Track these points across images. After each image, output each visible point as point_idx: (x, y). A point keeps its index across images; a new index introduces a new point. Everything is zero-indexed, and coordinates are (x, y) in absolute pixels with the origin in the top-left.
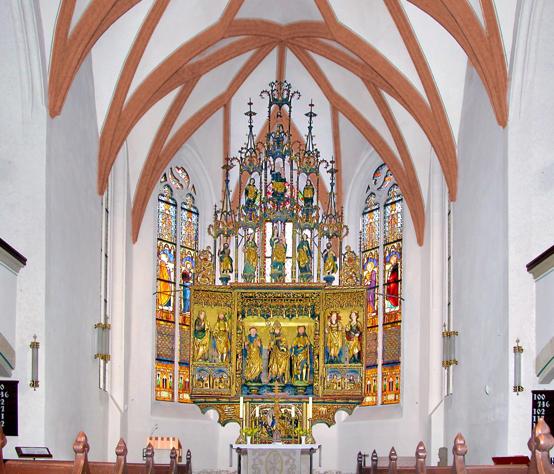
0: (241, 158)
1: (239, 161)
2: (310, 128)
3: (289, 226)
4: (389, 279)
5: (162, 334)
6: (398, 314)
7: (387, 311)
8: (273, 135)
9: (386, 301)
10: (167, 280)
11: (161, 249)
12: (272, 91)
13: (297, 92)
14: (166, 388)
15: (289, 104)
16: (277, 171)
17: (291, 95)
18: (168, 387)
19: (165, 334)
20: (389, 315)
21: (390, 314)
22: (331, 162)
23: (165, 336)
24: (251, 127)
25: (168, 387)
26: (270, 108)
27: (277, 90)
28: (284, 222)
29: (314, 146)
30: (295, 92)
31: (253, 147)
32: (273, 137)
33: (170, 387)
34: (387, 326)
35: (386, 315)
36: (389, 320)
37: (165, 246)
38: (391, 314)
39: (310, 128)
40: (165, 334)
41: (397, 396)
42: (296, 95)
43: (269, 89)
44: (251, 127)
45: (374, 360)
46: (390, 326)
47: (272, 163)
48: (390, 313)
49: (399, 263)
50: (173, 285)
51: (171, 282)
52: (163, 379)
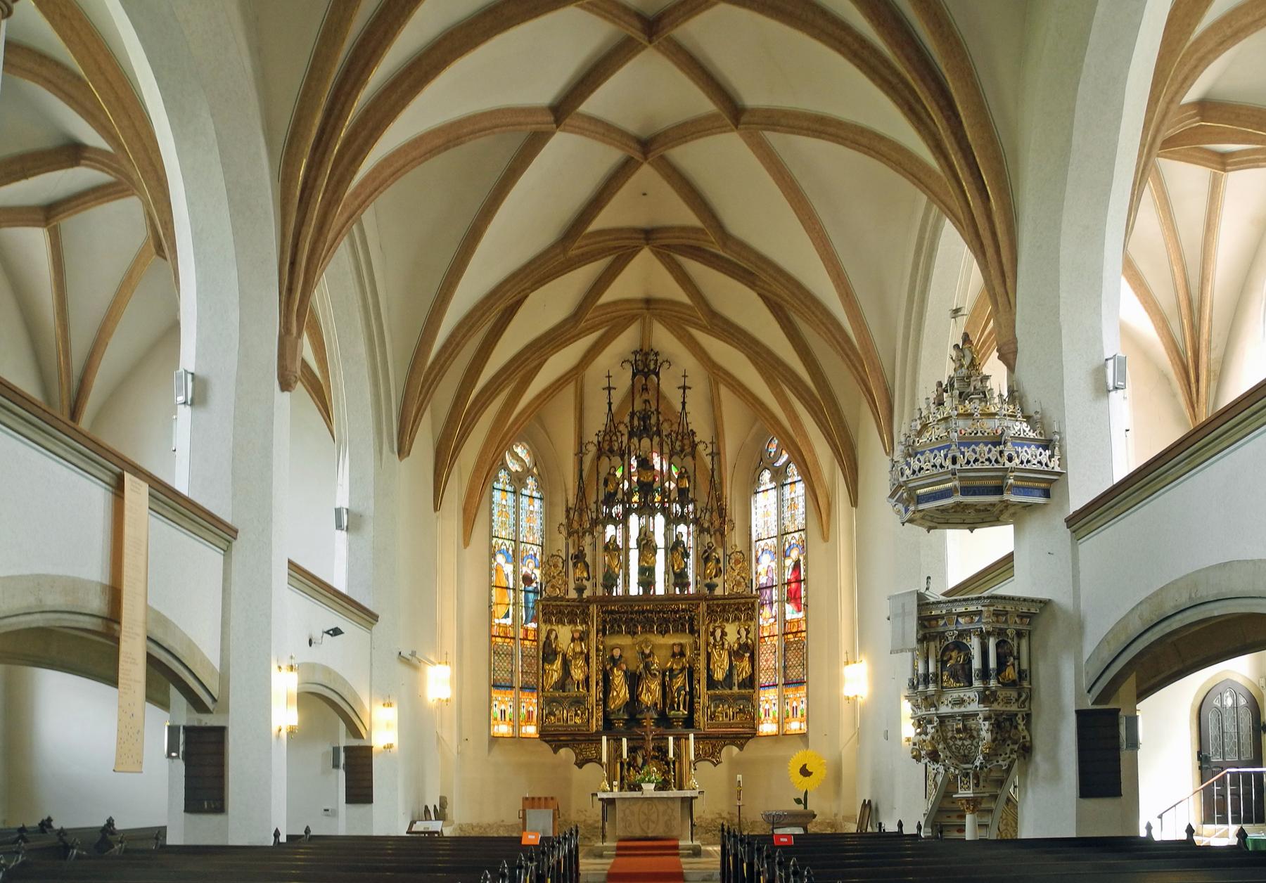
0: (599, 442)
1: (595, 445)
2: (684, 403)
3: (660, 520)
4: (789, 577)
5: (499, 653)
7: (788, 617)
8: (638, 414)
9: (786, 604)
10: (505, 586)
11: (497, 548)
12: (635, 360)
13: (667, 361)
14: (505, 720)
15: (657, 375)
17: (659, 364)
18: (507, 719)
19: (503, 653)
20: (790, 622)
21: (791, 622)
22: (710, 443)
23: (503, 656)
24: (610, 404)
25: (507, 719)
26: (633, 379)
27: (642, 361)
28: (652, 515)
29: (689, 425)
30: (664, 362)
31: (613, 429)
33: (510, 720)
37: (502, 544)
39: (684, 403)
40: (503, 653)
41: (802, 724)
42: (666, 365)
43: (632, 358)
44: (610, 404)
45: (774, 678)
47: (637, 447)
49: (801, 558)
50: (511, 591)
51: (510, 589)
52: (501, 711)
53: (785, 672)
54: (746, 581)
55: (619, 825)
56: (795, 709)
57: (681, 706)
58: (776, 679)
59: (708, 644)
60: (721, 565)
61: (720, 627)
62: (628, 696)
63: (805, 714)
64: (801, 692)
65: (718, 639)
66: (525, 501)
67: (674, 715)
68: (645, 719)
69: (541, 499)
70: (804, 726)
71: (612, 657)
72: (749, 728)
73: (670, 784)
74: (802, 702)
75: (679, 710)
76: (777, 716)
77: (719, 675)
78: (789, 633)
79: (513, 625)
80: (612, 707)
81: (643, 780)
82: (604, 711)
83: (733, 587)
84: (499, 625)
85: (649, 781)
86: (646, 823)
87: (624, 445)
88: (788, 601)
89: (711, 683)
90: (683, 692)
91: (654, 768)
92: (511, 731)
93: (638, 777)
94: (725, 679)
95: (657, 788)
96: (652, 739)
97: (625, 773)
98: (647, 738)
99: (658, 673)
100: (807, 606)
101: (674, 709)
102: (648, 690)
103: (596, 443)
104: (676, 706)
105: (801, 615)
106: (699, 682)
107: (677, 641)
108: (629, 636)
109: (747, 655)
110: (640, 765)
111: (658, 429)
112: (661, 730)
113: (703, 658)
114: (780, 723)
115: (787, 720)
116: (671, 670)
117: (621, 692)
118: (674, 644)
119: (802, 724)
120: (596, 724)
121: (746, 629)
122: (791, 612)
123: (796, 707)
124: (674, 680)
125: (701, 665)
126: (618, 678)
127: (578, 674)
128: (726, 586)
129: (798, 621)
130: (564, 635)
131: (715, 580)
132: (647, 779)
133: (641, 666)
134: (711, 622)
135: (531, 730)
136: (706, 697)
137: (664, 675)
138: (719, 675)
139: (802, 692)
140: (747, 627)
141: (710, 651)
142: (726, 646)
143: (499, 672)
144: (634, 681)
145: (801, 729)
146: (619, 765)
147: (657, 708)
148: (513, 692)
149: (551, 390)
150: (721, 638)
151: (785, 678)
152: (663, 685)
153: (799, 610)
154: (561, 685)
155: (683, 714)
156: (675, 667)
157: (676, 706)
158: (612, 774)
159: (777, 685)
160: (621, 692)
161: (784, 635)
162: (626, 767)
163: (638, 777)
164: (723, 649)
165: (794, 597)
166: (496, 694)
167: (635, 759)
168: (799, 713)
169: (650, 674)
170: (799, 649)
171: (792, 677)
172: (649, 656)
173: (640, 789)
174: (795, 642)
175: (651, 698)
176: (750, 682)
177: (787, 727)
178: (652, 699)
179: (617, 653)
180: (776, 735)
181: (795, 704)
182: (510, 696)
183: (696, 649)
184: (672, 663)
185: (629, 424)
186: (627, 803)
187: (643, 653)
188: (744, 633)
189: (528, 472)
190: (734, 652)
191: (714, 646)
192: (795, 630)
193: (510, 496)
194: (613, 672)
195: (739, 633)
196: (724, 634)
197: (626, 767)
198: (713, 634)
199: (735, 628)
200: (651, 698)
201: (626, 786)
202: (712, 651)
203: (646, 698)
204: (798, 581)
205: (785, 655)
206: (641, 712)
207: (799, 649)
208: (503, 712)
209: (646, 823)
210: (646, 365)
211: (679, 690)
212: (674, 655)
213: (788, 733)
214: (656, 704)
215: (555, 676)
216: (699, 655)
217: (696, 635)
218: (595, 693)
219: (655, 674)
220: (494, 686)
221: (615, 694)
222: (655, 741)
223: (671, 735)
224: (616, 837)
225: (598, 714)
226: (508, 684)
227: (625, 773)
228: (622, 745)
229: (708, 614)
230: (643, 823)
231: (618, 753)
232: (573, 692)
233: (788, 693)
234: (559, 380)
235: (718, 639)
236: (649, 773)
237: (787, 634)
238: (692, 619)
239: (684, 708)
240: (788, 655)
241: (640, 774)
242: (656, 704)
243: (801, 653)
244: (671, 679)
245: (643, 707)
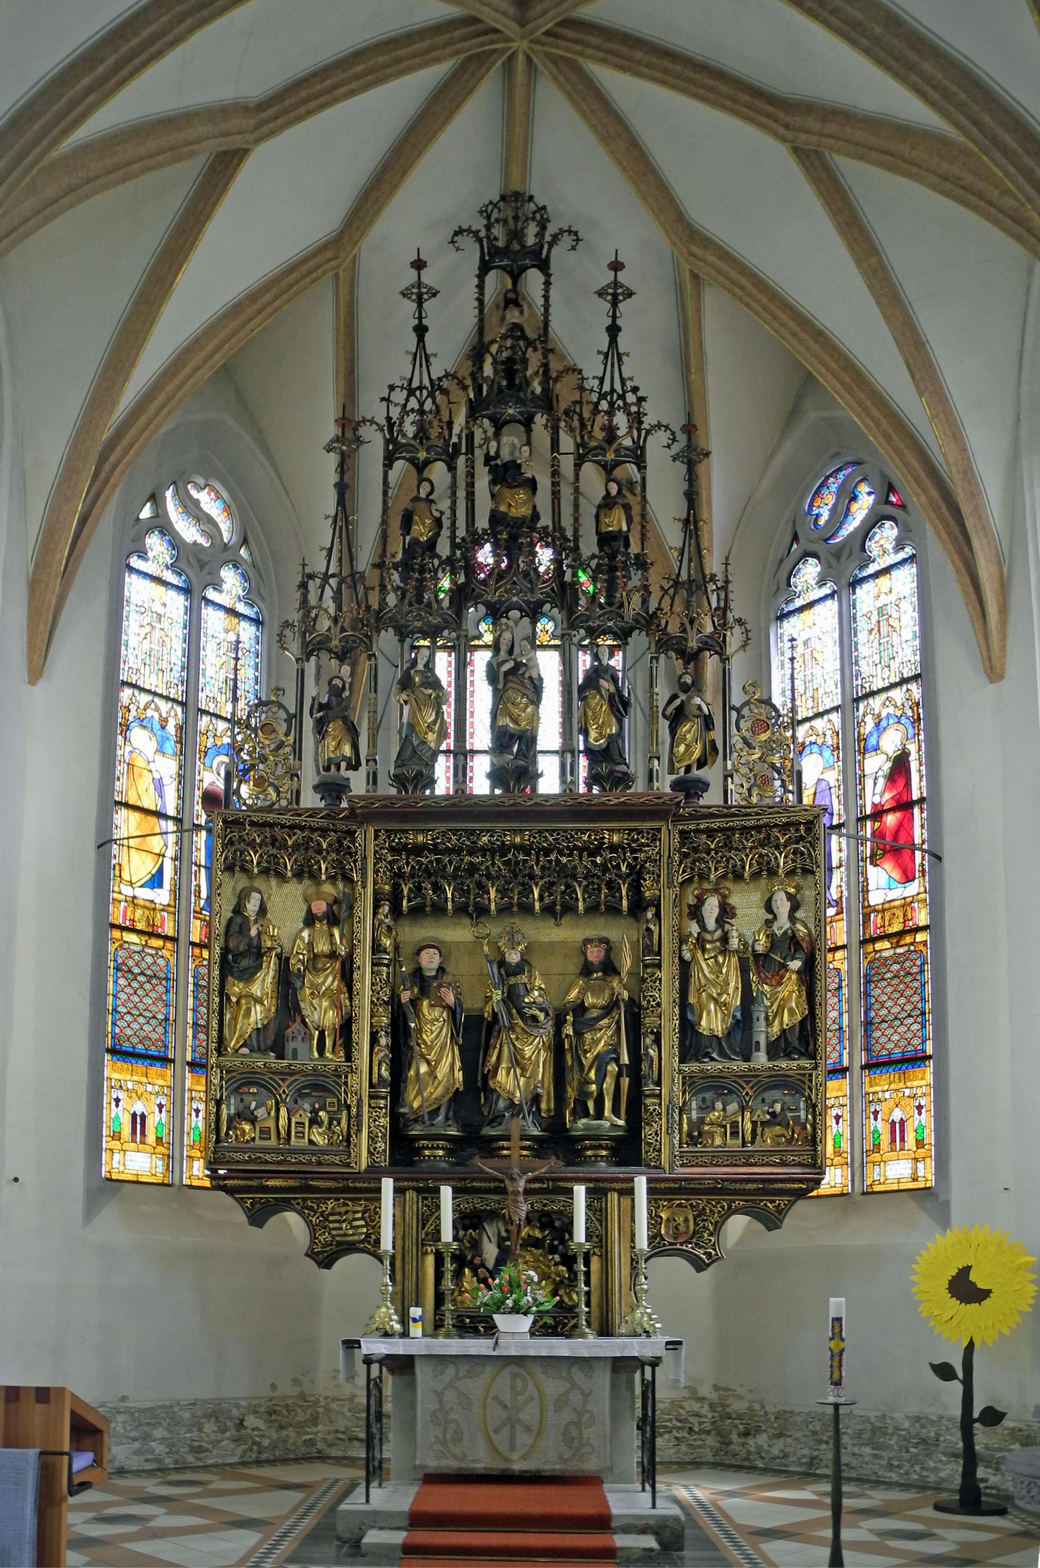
6: (916, 905)
16: (506, 456)
20: (883, 911)
32: (491, 354)
34: (879, 946)
35: (875, 911)
36: (884, 926)
38: (890, 909)
46: (886, 944)
48: (887, 906)
53: (868, 1035)
54: (784, 777)
55: (426, 1432)
56: (898, 1129)
57: (608, 1104)
58: (841, 1055)
59: (682, 941)
61: (716, 891)
62: (459, 1075)
63: (930, 1137)
64: (915, 1083)
65: (711, 923)
67: (587, 1128)
68: (507, 1138)
70: (927, 1172)
71: (418, 972)
73: (576, 1316)
74: (920, 1108)
75: (599, 1115)
76: (846, 1146)
78: (880, 938)
80: (416, 1105)
81: (498, 1306)
83: (749, 790)
85: (516, 1310)
86: (506, 1430)
87: (456, 430)
90: (612, 1068)
91: (532, 1273)
92: (160, 1169)
93: (485, 1296)
95: (541, 1329)
96: (527, 1192)
97: (448, 1283)
98: (510, 1188)
99: (541, 1016)
100: (939, 858)
101: (587, 1114)
102: (517, 1061)
103: (383, 422)
104: (591, 1104)
105: (913, 888)
106: (657, 1041)
107: (590, 933)
108: (467, 921)
110: (490, 1263)
111: (546, 390)
112: (550, 1165)
113: (668, 973)
114: (857, 1164)
115: (876, 1157)
116: (580, 1009)
118: (587, 941)
119: (921, 1166)
121: (790, 897)
123: (902, 1122)
124: (588, 1036)
125: (666, 993)
128: (730, 786)
129: (907, 904)
132: (509, 1303)
133: (497, 995)
134: (690, 881)
135: (197, 1171)
136: (678, 1079)
137: (559, 1023)
139: (924, 1078)
140: (792, 890)
141: (687, 956)
142: (734, 943)
143: (128, 1018)
145: (915, 1179)
146: (430, 1261)
147: (539, 1110)
148: (169, 1072)
149: (268, 296)
150: (720, 921)
151: (868, 1050)
152: (557, 1049)
153: (908, 877)
155: (614, 1126)
156: (590, 1000)
157: (591, 1104)
158: (411, 1285)
159: (847, 1069)
161: (864, 942)
162: (449, 1266)
163: (485, 1296)
164: (724, 952)
167: (476, 1246)
168: (910, 1138)
169: (522, 1015)
170: (909, 973)
171: (890, 1045)
172: (518, 969)
173: (491, 1330)
174: (896, 959)
175: (522, 1081)
177: (874, 1174)
178: (527, 1085)
179: (430, 960)
180: (842, 1195)
181: (897, 1115)
182: (161, 1082)
183: (648, 950)
184: (583, 992)
185: (468, 382)
186: (450, 1371)
187: (502, 963)
188: (783, 907)
190: (757, 956)
191: (701, 943)
192: (896, 927)
194: (418, 1013)
195: (769, 907)
196: (726, 912)
197: (449, 1266)
198: (696, 912)
199: (759, 895)
200: (522, 1081)
201: (449, 1321)
202: (693, 957)
203: (505, 1079)
205: (867, 994)
206: (497, 1119)
207: (909, 973)
208: (138, 1121)
209: (506, 1430)
210: (517, 235)
211: (600, 1062)
212: (587, 970)
213: (877, 1188)
214: (536, 1099)
216: (659, 966)
217: (650, 915)
219: (534, 1018)
220: (113, 1051)
221: (424, 1068)
222: (533, 1198)
223: (579, 1180)
224: (415, 1467)
226: (153, 1051)
227: (448, 1283)
228: (438, 1207)
229: (686, 856)
230: (496, 1431)
231: (430, 1228)
233: (877, 1089)
234: (291, 269)
235: (711, 923)
236: (513, 1285)
237: (873, 940)
238: (636, 876)
239: (616, 1111)
240: (876, 992)
241: (489, 1288)
242: (536, 1099)
243: (916, 984)
244: (579, 1034)
245: (502, 1104)
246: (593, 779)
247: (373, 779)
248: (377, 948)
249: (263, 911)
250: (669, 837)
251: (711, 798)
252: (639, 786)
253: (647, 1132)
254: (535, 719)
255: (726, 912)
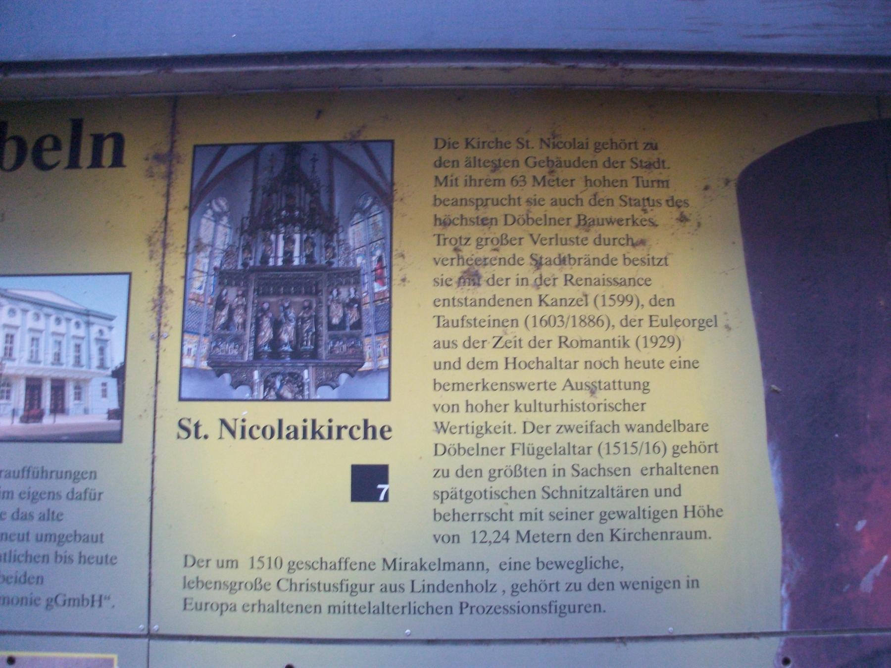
7: (376, 290)
21: (378, 293)
60: (336, 251)
62: (272, 335)
66: (220, 228)
69: (230, 228)
72: (358, 358)
75: (307, 345)
77: (335, 321)
79: (204, 294)
82: (255, 345)
84: (194, 293)
88: (376, 280)
89: (331, 327)
94: (340, 323)
102: (286, 331)
105: (385, 288)
109: (356, 305)
117: (267, 333)
120: (248, 355)
122: (377, 287)
125: (323, 313)
126: (266, 323)
127: (238, 319)
129: (384, 291)
130: (232, 295)
131: (332, 260)
138: (335, 321)
144: (277, 325)
154: (227, 326)
160: (267, 333)
165: (379, 278)
166: (186, 337)
176: (358, 325)
179: (266, 306)
189: (225, 213)
193: (212, 224)
196: (339, 294)
203: (285, 337)
204: (382, 268)
211: (307, 331)
215: (223, 320)
218: (249, 333)
225: (250, 348)
232: (235, 331)
238: (317, 285)
246: (307, 262)
247: (255, 262)
248: (253, 303)
249: (226, 294)
250: (324, 276)
251: (335, 266)
252: (318, 263)
253: (320, 350)
254: (293, 248)
255: (339, 294)
